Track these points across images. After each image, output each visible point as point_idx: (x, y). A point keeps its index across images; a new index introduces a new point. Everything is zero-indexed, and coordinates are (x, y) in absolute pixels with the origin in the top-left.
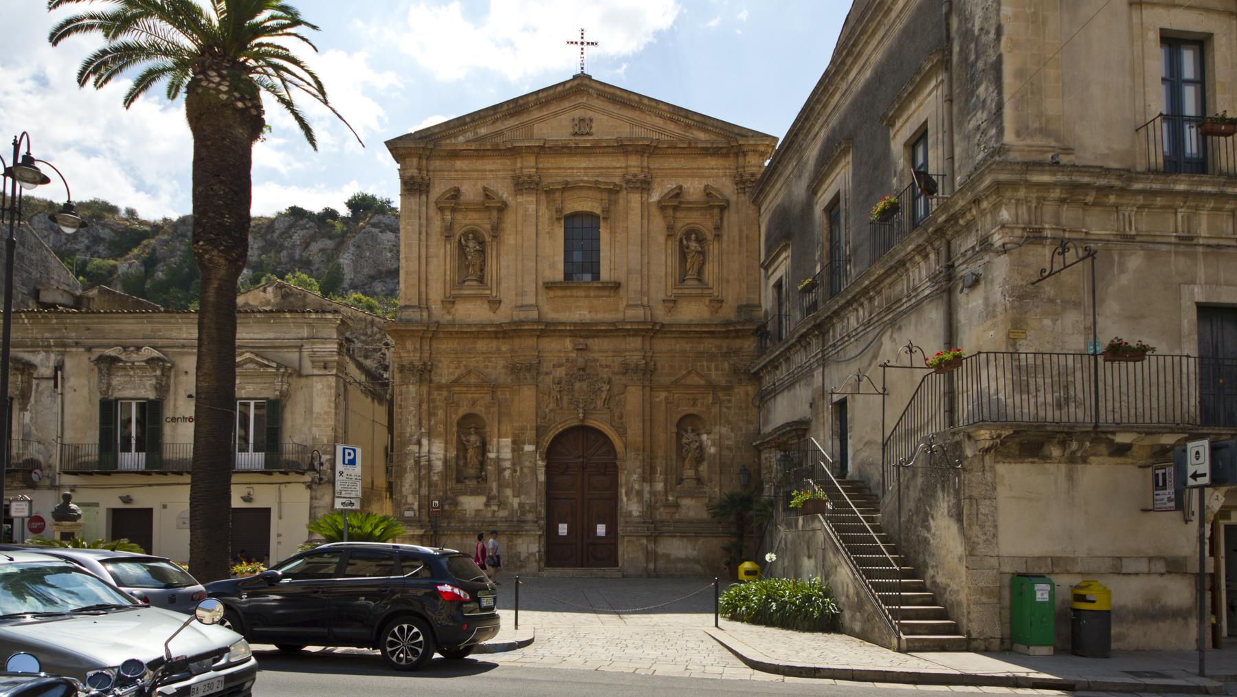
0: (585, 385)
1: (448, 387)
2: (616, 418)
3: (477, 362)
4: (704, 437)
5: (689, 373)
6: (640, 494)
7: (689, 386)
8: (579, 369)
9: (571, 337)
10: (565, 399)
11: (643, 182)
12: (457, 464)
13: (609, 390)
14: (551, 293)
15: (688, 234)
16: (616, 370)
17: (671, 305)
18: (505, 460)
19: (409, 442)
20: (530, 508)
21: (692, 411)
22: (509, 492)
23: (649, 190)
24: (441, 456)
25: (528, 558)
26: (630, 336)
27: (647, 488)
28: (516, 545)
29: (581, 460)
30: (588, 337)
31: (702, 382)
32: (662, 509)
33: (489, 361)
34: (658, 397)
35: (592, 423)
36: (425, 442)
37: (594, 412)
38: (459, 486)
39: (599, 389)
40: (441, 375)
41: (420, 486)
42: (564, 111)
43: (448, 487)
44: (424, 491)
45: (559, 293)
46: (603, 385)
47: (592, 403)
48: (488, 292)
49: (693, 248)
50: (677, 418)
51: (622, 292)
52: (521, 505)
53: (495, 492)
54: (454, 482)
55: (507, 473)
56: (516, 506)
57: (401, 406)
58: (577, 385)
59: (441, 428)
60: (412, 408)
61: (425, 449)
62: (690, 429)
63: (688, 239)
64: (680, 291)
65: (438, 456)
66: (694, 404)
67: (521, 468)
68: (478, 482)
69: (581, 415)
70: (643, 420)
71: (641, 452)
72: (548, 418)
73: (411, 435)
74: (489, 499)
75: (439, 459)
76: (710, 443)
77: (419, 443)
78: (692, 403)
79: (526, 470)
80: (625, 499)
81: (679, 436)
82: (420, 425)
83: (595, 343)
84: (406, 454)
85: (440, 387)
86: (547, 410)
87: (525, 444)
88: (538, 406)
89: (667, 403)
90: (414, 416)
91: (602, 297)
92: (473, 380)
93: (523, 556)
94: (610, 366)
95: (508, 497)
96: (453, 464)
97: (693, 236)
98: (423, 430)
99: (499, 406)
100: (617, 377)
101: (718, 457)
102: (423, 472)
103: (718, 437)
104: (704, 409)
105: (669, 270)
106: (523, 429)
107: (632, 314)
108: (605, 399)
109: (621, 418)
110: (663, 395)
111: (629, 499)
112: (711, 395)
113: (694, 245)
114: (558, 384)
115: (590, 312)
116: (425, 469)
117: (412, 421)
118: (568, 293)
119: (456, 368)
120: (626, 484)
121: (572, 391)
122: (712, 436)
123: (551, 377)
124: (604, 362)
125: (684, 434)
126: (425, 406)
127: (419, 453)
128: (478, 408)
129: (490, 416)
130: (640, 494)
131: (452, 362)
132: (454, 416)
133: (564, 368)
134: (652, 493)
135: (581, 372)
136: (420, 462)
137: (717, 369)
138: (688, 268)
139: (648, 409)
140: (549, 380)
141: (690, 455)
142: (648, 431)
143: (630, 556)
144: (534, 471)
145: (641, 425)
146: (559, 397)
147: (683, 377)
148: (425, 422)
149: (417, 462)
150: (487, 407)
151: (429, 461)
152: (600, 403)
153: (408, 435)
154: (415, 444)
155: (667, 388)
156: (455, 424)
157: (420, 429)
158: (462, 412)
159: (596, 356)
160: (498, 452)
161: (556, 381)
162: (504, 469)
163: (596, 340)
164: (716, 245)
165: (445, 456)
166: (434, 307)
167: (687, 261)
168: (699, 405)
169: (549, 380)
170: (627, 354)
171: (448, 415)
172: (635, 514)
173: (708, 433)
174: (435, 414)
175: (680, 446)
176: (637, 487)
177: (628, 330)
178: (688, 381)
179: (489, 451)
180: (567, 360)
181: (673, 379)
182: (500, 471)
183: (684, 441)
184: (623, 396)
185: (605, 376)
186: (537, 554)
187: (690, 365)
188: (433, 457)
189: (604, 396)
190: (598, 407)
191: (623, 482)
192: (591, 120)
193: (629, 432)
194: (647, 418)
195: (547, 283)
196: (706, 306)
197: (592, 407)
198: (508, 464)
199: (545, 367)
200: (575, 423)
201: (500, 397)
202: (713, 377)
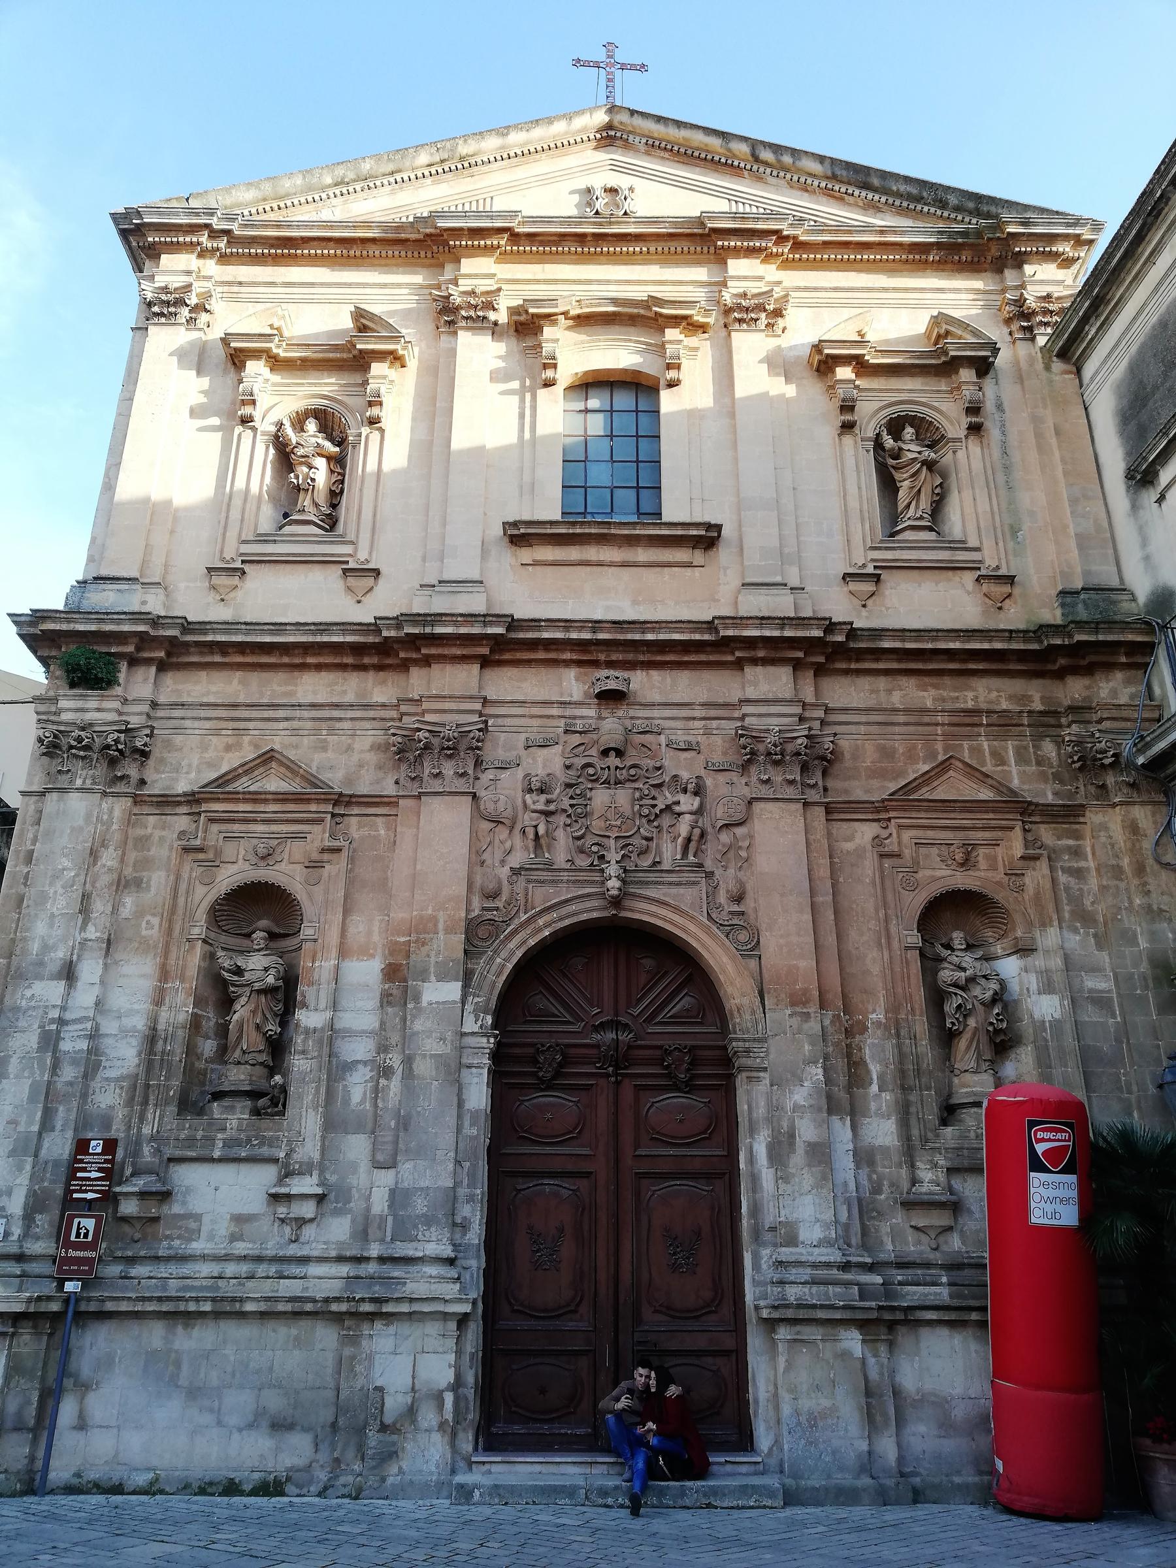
0: (623, 797)
1: (193, 799)
2: (722, 898)
4: (1010, 967)
5: (943, 767)
6: (820, 1153)
7: (946, 805)
8: (605, 753)
9: (580, 663)
10: (562, 840)
12: (191, 1050)
13: (699, 812)
14: (527, 554)
15: (895, 426)
16: (717, 758)
17: (869, 587)
18: (350, 1033)
21: (962, 880)
25: (411, 1412)
26: (755, 661)
28: (370, 1358)
30: (632, 666)
31: (986, 794)
32: (899, 1218)
33: (332, 731)
34: (850, 839)
35: (642, 912)
36: (90, 970)
37: (652, 877)
38: (190, 1127)
39: (668, 808)
41: (47, 1124)
43: (146, 1130)
46: (682, 798)
47: (643, 852)
49: (911, 456)
50: (917, 902)
51: (724, 554)
52: (398, 1197)
53: (310, 1150)
54: (172, 1109)
55: (357, 1087)
56: (379, 1204)
57: (29, 858)
58: (600, 797)
59: (152, 928)
62: (958, 938)
63: (897, 435)
64: (889, 555)
65: (128, 1022)
66: (967, 863)
69: (614, 884)
70: (813, 906)
72: (504, 896)
76: (1032, 981)
77: (69, 973)
78: (959, 857)
79: (423, 1067)
80: (767, 1176)
81: (930, 963)
83: (643, 683)
85: (166, 802)
86: (504, 872)
88: (477, 859)
89: (882, 856)
92: (274, 783)
93: (394, 1404)
95: (354, 1167)
96: (178, 1053)
97: (909, 432)
98: (92, 933)
99: (352, 860)
100: (722, 778)
101: (1068, 1028)
102: (69, 1073)
103: (1057, 962)
104: (999, 876)
105: (853, 503)
106: (422, 929)
107: (755, 604)
108: (689, 840)
109: (739, 899)
110: (865, 832)
111: (783, 1177)
112: (1018, 831)
113: (912, 449)
114: (542, 791)
115: (635, 602)
116: (74, 1062)
117: (61, 902)
118: (573, 553)
119: (228, 748)
120: (769, 1120)
121: (579, 813)
122: (1038, 961)
123: (520, 772)
124: (681, 738)
125: (945, 953)
126: (109, 858)
127: (64, 1008)
128: (283, 866)
129: (318, 891)
130: (820, 1153)
131: (217, 732)
133: (558, 749)
134: (864, 1157)
135: (612, 760)
136: (58, 1038)
137: (1021, 759)
138: (901, 506)
139: (823, 872)
140: (511, 782)
141: (972, 1022)
142: (831, 940)
143: (806, 1404)
146: (541, 830)
147: (926, 779)
148: (100, 907)
149: (50, 1041)
150: (314, 865)
152: (669, 852)
153: (35, 947)
154: (58, 976)
155: (878, 811)
156: (201, 916)
157: (83, 928)
158: (229, 877)
160: (335, 1006)
161: (535, 784)
162: (349, 1067)
167: (897, 490)
168: (983, 864)
169: (511, 782)
170: (748, 709)
171: (183, 887)
172: (810, 1233)
173: (1024, 950)
174: (138, 884)
175: (937, 997)
176: (807, 1131)
178: (942, 792)
179: (304, 1005)
181: (893, 786)
183: (946, 975)
184: (740, 831)
185: (685, 775)
186: (449, 1398)
187: (939, 747)
189: (683, 828)
190: (666, 865)
191: (761, 1111)
193: (770, 944)
194: (825, 898)
195: (515, 524)
196: (969, 593)
197: (646, 863)
198: (359, 1050)
199: (499, 748)
200: (591, 911)
201: (356, 835)
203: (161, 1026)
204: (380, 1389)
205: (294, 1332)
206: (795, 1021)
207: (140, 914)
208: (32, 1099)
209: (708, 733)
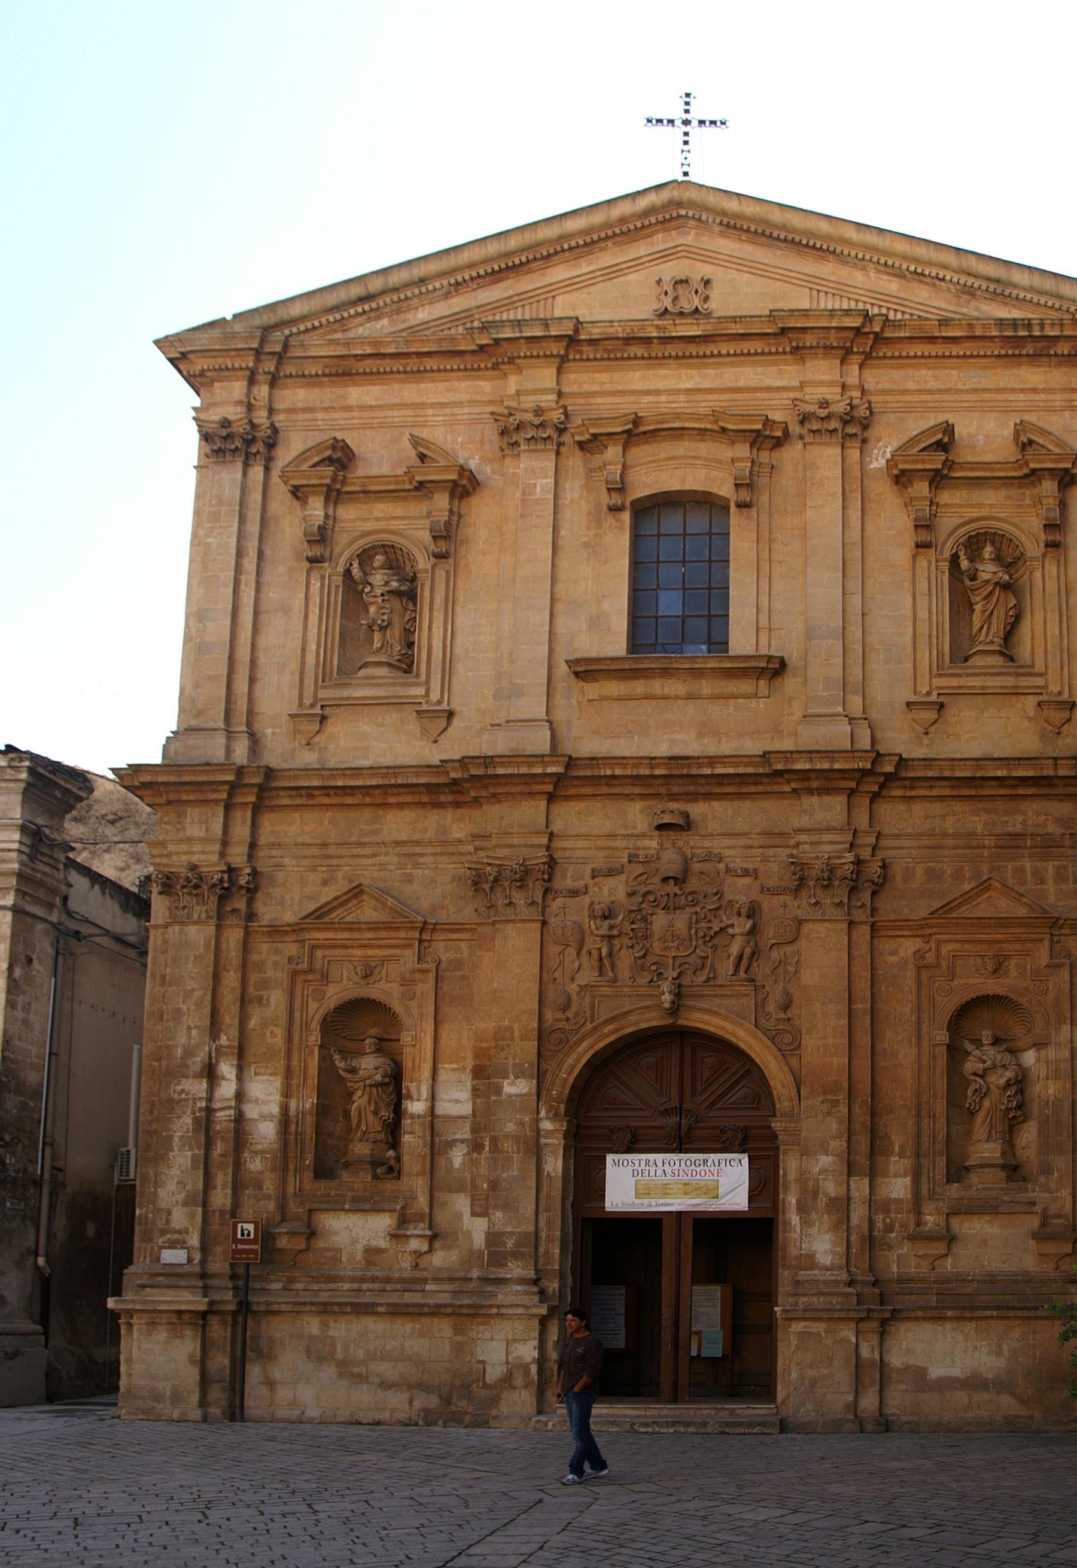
0: (681, 921)
1: (298, 928)
2: (771, 1008)
3: (382, 866)
5: (984, 887)
6: (841, 1206)
7: (981, 923)
8: (665, 880)
9: (643, 797)
10: (626, 959)
11: (847, 419)
13: (753, 932)
14: (592, 690)
15: (974, 543)
16: (772, 882)
17: (930, 715)
19: (174, 1074)
20: (518, 1244)
21: (993, 986)
22: (462, 1203)
23: (864, 441)
24: (275, 1109)
26: (810, 791)
27: (860, 1187)
29: (674, 1120)
30: (693, 797)
31: (1022, 912)
32: (905, 1249)
33: (416, 865)
35: (697, 1019)
36: (227, 1069)
37: (706, 991)
38: (322, 1186)
40: (282, 902)
41: (208, 1185)
42: (636, 264)
44: (221, 1198)
45: (613, 688)
46: (735, 920)
48: (421, 691)
49: (985, 576)
50: (948, 1006)
51: (790, 684)
52: (494, 1238)
54: (309, 1175)
55: (458, 1157)
56: (479, 1240)
58: (660, 921)
60: (191, 985)
61: (227, 1089)
63: (975, 556)
64: (954, 682)
65: (266, 1109)
66: (998, 970)
67: (494, 1140)
68: (375, 1177)
71: (842, 1096)
72: (574, 1008)
73: (189, 1053)
74: (403, 1220)
75: (269, 1117)
77: (211, 1074)
78: (990, 966)
80: (795, 1219)
81: (955, 1052)
82: (215, 1028)
84: (170, 1101)
85: (276, 931)
86: (573, 988)
87: (506, 1077)
90: (199, 1004)
91: (734, 697)
92: (368, 912)
94: (755, 874)
95: (459, 1216)
97: (988, 551)
98: (224, 1040)
105: (923, 629)
108: (740, 958)
109: (786, 1007)
112: (1046, 943)
113: (988, 570)
115: (700, 735)
116: (223, 1140)
117: (195, 1018)
118: (639, 687)
119: (325, 882)
120: (799, 1180)
122: (1051, 1053)
123: (587, 900)
124: (738, 864)
125: (969, 1047)
128: (382, 985)
129: (414, 1004)
131: (313, 868)
132: (313, 1006)
133: (623, 877)
135: (672, 888)
137: (1060, 876)
138: (976, 628)
139: (863, 984)
141: (987, 1103)
144: (536, 1151)
145: (844, 1022)
147: (968, 897)
150: (405, 982)
151: (240, 1118)
152: (726, 968)
154: (198, 1076)
155: (920, 929)
156: (315, 1026)
158: (335, 995)
159: (717, 845)
160: (433, 1097)
163: (716, 805)
164: (1051, 569)
165: (285, 1109)
166: (269, 731)
167: (973, 611)
168: (1013, 972)
170: (804, 838)
171: (298, 1004)
173: (1040, 1045)
177: (805, 774)
178: (982, 909)
179: (410, 1097)
180: (632, 859)
181: (938, 904)
182: (436, 1148)
183: (971, 1066)
184: (788, 949)
187: (985, 868)
188: (251, 1111)
189: (735, 949)
191: (792, 1175)
192: (707, 283)
193: (809, 1043)
194: (862, 1006)
195: (578, 661)
196: (1030, 719)
200: (652, 1020)
202: (1052, 900)
203: (292, 1112)
204: (483, 1362)
205: (418, 1326)
206: (825, 1107)
207: (264, 1025)
208: (194, 1167)
209: (765, 860)
